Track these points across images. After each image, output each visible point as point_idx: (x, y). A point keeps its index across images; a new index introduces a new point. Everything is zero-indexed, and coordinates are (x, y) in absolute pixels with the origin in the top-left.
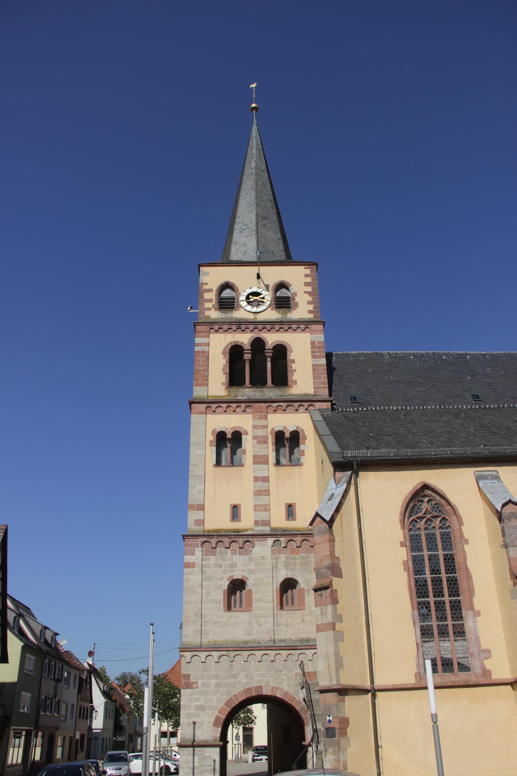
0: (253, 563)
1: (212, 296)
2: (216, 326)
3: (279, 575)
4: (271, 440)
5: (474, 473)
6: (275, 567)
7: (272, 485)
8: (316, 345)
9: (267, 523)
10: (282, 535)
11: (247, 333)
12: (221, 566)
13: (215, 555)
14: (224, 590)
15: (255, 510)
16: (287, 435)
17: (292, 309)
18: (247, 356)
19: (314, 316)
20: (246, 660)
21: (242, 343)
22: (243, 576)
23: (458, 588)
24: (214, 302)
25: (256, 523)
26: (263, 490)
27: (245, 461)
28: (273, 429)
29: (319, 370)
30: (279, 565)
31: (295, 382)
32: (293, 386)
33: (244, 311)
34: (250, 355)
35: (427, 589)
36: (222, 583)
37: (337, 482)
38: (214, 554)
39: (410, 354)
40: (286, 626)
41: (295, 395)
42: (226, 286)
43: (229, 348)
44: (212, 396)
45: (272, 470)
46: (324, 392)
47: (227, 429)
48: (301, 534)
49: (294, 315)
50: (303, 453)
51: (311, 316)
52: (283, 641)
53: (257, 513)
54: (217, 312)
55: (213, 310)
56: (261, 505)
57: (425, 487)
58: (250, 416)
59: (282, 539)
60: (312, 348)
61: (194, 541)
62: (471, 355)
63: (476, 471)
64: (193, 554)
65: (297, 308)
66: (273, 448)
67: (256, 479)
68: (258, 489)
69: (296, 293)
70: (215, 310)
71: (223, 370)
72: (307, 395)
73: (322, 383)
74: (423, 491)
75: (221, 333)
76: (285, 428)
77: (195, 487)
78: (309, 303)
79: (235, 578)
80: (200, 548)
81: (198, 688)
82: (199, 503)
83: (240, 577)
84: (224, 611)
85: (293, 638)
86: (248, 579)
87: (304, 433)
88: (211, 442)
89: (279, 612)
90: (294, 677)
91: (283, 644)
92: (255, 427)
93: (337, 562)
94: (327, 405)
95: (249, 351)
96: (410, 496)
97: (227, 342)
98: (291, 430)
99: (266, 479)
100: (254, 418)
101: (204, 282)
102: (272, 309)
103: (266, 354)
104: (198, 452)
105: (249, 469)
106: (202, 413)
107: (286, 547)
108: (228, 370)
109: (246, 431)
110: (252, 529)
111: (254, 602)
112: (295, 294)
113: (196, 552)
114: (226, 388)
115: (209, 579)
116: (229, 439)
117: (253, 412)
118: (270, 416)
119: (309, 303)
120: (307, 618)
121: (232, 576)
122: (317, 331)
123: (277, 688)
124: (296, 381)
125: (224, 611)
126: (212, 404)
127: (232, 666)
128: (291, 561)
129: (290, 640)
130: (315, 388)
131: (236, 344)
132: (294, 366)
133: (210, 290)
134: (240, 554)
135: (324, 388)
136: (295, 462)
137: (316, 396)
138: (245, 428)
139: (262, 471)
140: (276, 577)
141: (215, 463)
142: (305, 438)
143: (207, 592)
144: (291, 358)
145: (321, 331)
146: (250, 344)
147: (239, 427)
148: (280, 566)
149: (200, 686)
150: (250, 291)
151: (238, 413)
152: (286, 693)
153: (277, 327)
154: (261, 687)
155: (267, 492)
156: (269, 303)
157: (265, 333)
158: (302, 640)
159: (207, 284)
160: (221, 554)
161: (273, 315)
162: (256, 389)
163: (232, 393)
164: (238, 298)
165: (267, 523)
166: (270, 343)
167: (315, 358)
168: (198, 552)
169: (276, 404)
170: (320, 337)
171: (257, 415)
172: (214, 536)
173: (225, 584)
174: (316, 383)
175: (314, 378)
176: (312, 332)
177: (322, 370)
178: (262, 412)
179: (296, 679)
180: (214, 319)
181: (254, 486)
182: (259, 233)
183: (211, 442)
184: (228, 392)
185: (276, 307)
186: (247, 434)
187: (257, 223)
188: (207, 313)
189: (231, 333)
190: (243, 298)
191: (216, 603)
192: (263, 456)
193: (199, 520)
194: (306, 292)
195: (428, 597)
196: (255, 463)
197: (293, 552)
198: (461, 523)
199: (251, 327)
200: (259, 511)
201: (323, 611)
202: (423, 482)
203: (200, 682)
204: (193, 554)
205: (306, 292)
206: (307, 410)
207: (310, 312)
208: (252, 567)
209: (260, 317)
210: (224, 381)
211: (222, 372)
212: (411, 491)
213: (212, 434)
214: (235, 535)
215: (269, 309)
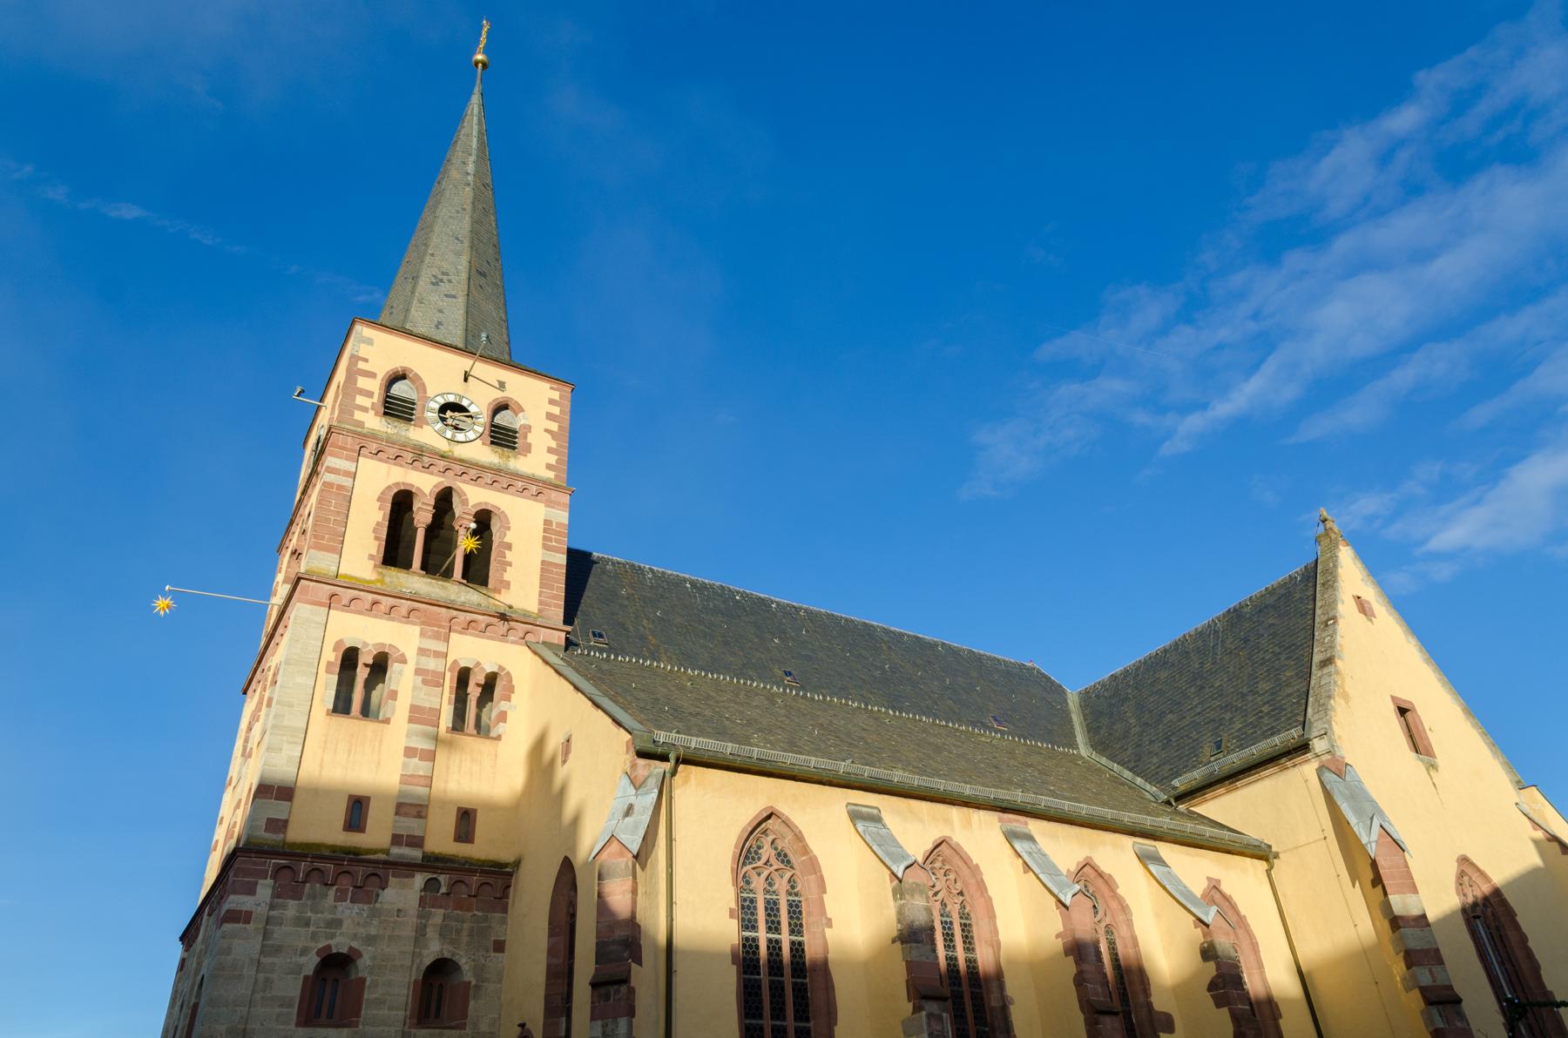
1: (375, 386)
3: (425, 952)
4: (449, 682)
6: (421, 932)
10: (444, 870)
14: (306, 978)
15: (397, 813)
22: (351, 948)
23: (807, 1005)
24: (375, 400)
25: (397, 840)
28: (455, 662)
31: (507, 585)
33: (428, 434)
35: (761, 1001)
36: (303, 960)
37: (637, 785)
38: (297, 895)
39: (685, 580)
44: (346, 576)
48: (483, 872)
49: (519, 464)
50: (503, 717)
51: (551, 475)
53: (402, 819)
58: (417, 629)
59: (443, 878)
60: (545, 531)
62: (778, 604)
64: (251, 890)
73: (555, 597)
76: (478, 664)
80: (270, 882)
83: (345, 950)
84: (298, 1024)
86: (360, 955)
88: (329, 663)
92: (422, 652)
97: (390, 483)
100: (422, 634)
106: (321, 604)
109: (403, 655)
110: (387, 852)
112: (528, 428)
113: (259, 889)
115: (277, 950)
117: (423, 623)
119: (550, 450)
121: (329, 946)
124: (508, 583)
125: (298, 1024)
126: (340, 592)
130: (541, 603)
132: (509, 556)
133: (372, 375)
135: (556, 606)
140: (420, 954)
142: (511, 689)
143: (267, 980)
148: (431, 932)
150: (451, 399)
151: (393, 620)
153: (488, 478)
156: (480, 430)
159: (366, 360)
160: (313, 897)
161: (484, 453)
163: (387, 579)
165: (416, 842)
168: (265, 889)
170: (562, 517)
172: (306, 856)
173: (311, 962)
176: (550, 504)
181: (405, 765)
183: (329, 663)
186: (404, 661)
188: (358, 415)
191: (281, 1006)
195: (761, 1017)
196: (411, 720)
197: (459, 906)
198: (822, 888)
199: (442, 464)
200: (406, 815)
201: (611, 1026)
204: (251, 890)
207: (549, 467)
208: (373, 931)
209: (461, 451)
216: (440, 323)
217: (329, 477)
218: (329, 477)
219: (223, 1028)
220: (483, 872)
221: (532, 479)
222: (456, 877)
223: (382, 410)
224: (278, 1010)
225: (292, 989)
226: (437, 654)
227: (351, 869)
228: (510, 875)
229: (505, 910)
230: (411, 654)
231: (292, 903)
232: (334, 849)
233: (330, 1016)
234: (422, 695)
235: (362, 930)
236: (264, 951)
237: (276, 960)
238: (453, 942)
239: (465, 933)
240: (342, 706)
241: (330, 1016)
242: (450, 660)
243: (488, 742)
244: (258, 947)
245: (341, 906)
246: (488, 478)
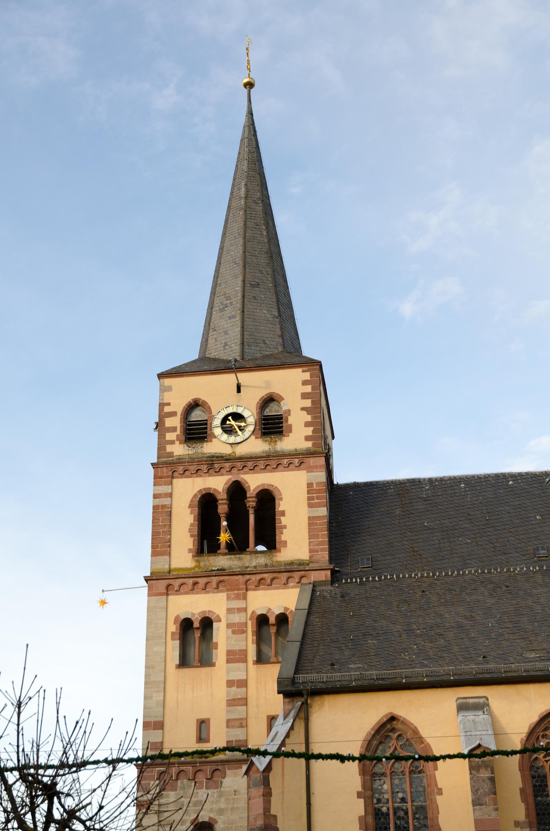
0: (223, 800)
2: (181, 468)
4: (250, 628)
5: (456, 701)
8: (315, 488)
11: (222, 475)
13: (176, 790)
15: (228, 727)
17: (284, 436)
18: (223, 508)
19: (314, 445)
21: (215, 489)
22: (210, 818)
26: (239, 699)
28: (253, 612)
29: (316, 524)
32: (282, 549)
33: (219, 443)
34: (226, 506)
42: (195, 405)
46: (324, 556)
47: (193, 614)
51: (309, 444)
53: (231, 730)
55: (177, 443)
56: (235, 720)
57: (393, 718)
63: (458, 698)
65: (290, 434)
66: (253, 640)
67: (230, 683)
69: (289, 411)
70: (180, 443)
71: (189, 532)
72: (301, 563)
74: (389, 726)
77: (152, 697)
78: (307, 424)
83: (206, 820)
86: (216, 822)
92: (230, 611)
93: (272, 821)
94: (326, 575)
96: (373, 732)
98: (277, 613)
99: (243, 684)
100: (228, 598)
101: (165, 402)
102: (256, 438)
105: (222, 668)
106: (161, 594)
108: (197, 531)
109: (218, 616)
112: (289, 412)
114: (193, 556)
117: (228, 590)
119: (307, 424)
122: (316, 467)
124: (285, 542)
130: (311, 551)
132: (284, 520)
133: (173, 414)
135: (322, 550)
137: (312, 562)
138: (217, 612)
139: (238, 672)
141: (177, 662)
144: (281, 509)
145: (321, 466)
146: (225, 491)
147: (209, 611)
151: (208, 592)
155: (244, 702)
157: (246, 473)
159: (169, 404)
160: (183, 788)
161: (257, 446)
162: (233, 556)
164: (211, 423)
166: (252, 489)
167: (311, 507)
169: (258, 577)
174: (312, 544)
175: (310, 537)
176: (310, 469)
177: (320, 524)
181: (228, 693)
182: (246, 313)
183: (173, 633)
184: (197, 561)
186: (220, 620)
187: (243, 296)
189: (201, 476)
190: (217, 422)
192: (240, 650)
193: (157, 743)
194: (303, 409)
196: (228, 661)
199: (227, 465)
200: (233, 727)
202: (391, 713)
205: (303, 409)
207: (307, 438)
208: (222, 806)
209: (241, 451)
210: (191, 547)
211: (189, 534)
212: (374, 726)
213: (175, 623)
214: (200, 763)
215: (253, 437)
216: (226, 344)
223: (183, 438)
226: (240, 610)
227: (202, 768)
240: (184, 662)
242: (249, 612)
246: (261, 464)
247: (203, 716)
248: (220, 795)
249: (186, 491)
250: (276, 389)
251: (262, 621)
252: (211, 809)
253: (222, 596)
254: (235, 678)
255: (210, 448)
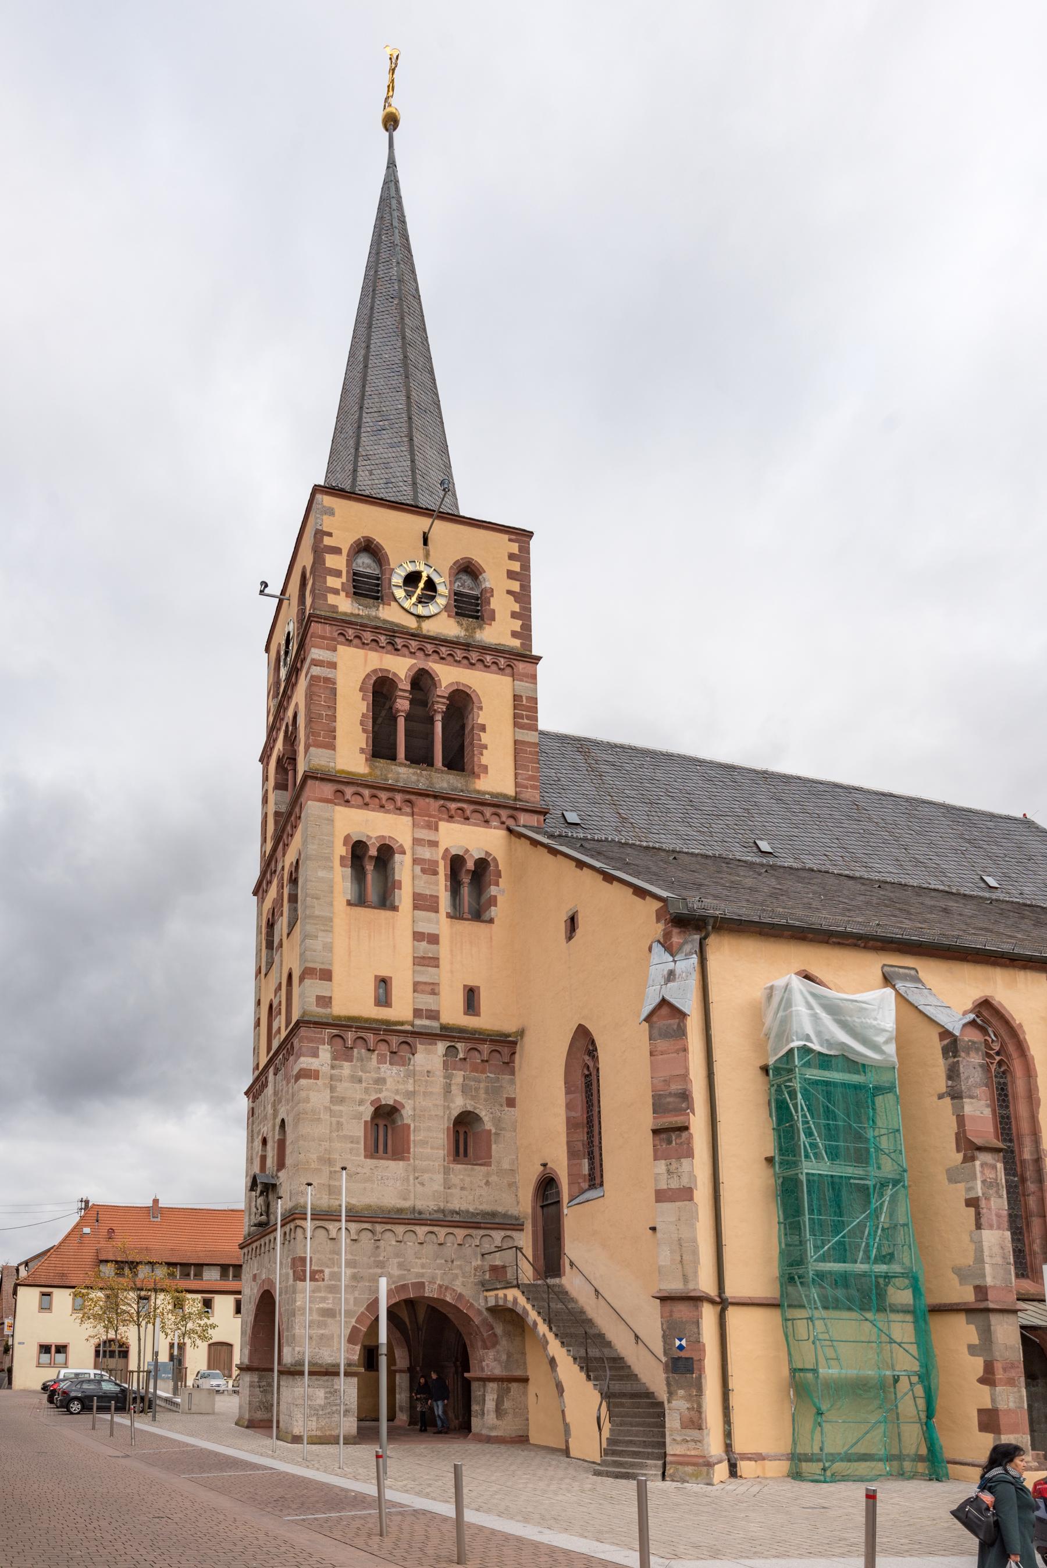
4: (443, 869)
6: (447, 1090)
7: (444, 951)
9: (434, 1015)
10: (460, 1039)
11: (404, 656)
12: (360, 1081)
13: (352, 1061)
14: (366, 1122)
16: (470, 865)
18: (403, 705)
20: (400, 1238)
21: (395, 674)
22: (395, 1101)
24: (344, 579)
25: (417, 1013)
27: (400, 902)
28: (447, 850)
29: (525, 752)
30: (453, 1088)
33: (399, 610)
36: (362, 1108)
40: (462, 1189)
41: (485, 793)
43: (372, 682)
44: (343, 771)
45: (441, 923)
48: (492, 1041)
50: (493, 901)
51: (516, 643)
52: (457, 1213)
54: (349, 600)
56: (425, 983)
59: (459, 1045)
60: (515, 707)
61: (318, 1033)
64: (315, 1055)
67: (418, 936)
68: (421, 954)
72: (505, 796)
75: (357, 647)
76: (467, 851)
78: (514, 615)
79: (383, 1103)
80: (327, 1047)
81: (323, 1280)
82: (323, 967)
83: (391, 1102)
84: (366, 1157)
85: (471, 1210)
86: (404, 1107)
87: (497, 865)
88: (342, 857)
89: (451, 1166)
90: (473, 1272)
91: (457, 1218)
92: (416, 841)
95: (407, 695)
97: (369, 669)
99: (434, 939)
103: (436, 707)
104: (321, 874)
107: (465, 1059)
109: (401, 846)
111: (412, 1146)
114: (367, 760)
115: (341, 1100)
116: (371, 857)
118: (443, 825)
119: (514, 615)
120: (493, 1179)
121: (379, 1099)
123: (447, 1288)
125: (366, 1157)
126: (343, 787)
127: (378, 1247)
128: (473, 1083)
129: (468, 1212)
130: (517, 785)
131: (385, 674)
132: (485, 738)
134: (391, 1064)
136: (479, 914)
138: (401, 841)
139: (429, 922)
140: (448, 1107)
143: (338, 1123)
144: (480, 721)
148: (455, 1090)
149: (326, 1277)
151: (388, 812)
152: (460, 1296)
153: (459, 654)
154: (423, 1283)
155: (433, 962)
158: (484, 1214)
165: (434, 1015)
166: (444, 685)
171: (421, 820)
172: (351, 1027)
173: (368, 1111)
177: (531, 753)
178: (430, 816)
179: (475, 1275)
180: (345, 614)
183: (342, 857)
184: (370, 767)
185: (457, 614)
186: (404, 853)
189: (376, 651)
190: (397, 579)
194: (509, 592)
196: (416, 907)
197: (475, 1069)
200: (423, 992)
203: (327, 1271)
204: (315, 1055)
205: (509, 592)
206: (503, 823)
207: (515, 634)
208: (411, 1088)
209: (429, 628)
214: (385, 1030)
215: (445, 614)
217: (316, 671)
218: (316, 671)
219: (314, 1157)
220: (492, 1041)
221: (497, 651)
222: (470, 1046)
224: (350, 1145)
225: (358, 1130)
228: (515, 1043)
229: (513, 1073)
230: (407, 844)
231: (346, 1064)
232: (367, 1020)
233: (385, 1151)
234: (422, 884)
235: (401, 1087)
236: (334, 1100)
237: (341, 1108)
238: (473, 1098)
239: (482, 1091)
240: (360, 901)
241: (385, 1151)
243: (483, 925)
244: (328, 1097)
245: (385, 1067)
247: (384, 973)
248: (407, 1076)
249: (352, 667)
250: (479, 558)
251: (456, 863)
252: (397, 1090)
253: (407, 820)
254: (426, 931)
255: (389, 613)
